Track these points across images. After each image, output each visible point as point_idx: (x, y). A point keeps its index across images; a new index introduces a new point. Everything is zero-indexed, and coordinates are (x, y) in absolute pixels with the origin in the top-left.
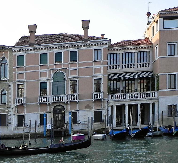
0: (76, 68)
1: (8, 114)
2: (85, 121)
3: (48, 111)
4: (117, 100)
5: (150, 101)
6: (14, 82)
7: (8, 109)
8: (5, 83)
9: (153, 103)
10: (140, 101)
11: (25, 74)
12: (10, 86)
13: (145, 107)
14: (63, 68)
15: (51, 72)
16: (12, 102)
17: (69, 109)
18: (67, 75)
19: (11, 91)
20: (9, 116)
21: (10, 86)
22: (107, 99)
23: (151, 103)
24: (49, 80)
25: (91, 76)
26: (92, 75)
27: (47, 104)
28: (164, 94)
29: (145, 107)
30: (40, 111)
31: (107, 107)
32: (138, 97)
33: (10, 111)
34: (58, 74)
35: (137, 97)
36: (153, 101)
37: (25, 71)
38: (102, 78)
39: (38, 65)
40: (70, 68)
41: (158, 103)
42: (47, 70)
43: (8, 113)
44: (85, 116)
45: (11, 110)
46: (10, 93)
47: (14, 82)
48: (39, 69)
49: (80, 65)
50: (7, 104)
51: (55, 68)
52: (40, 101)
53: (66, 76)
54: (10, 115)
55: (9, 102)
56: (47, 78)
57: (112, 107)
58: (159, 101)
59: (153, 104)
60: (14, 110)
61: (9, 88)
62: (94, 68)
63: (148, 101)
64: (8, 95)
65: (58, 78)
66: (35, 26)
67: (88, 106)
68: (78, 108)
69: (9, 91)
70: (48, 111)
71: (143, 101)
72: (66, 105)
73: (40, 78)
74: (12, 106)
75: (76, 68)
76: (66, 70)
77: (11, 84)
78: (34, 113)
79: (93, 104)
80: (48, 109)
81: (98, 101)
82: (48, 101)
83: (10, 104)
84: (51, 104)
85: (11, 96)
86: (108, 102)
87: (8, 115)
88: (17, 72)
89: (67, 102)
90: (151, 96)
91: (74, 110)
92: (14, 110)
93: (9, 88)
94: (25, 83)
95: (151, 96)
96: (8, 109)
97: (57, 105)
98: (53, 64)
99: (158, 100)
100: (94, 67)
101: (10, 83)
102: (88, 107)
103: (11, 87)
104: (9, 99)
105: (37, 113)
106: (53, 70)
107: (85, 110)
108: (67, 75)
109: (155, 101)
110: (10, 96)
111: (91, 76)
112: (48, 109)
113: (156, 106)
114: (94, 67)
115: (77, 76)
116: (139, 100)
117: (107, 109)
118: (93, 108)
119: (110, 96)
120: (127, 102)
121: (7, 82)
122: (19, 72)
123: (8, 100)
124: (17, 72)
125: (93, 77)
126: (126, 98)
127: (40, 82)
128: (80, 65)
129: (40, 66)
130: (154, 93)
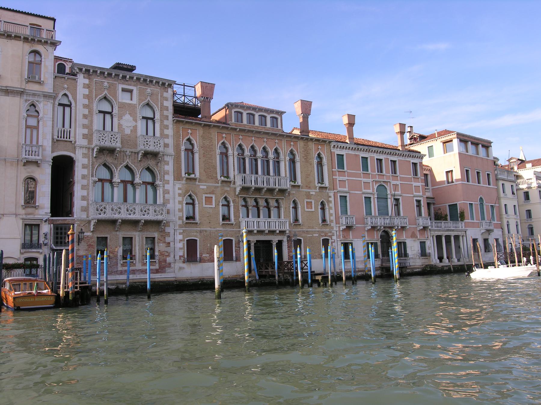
6: (335, 191)
12: (330, 197)
14: (385, 180)
16: (334, 221)
19: (332, 205)
24: (373, 194)
26: (413, 194)
33: (334, 235)
37: (346, 178)
42: (370, 180)
43: (331, 236)
46: (330, 208)
47: (335, 191)
49: (402, 179)
51: (377, 179)
53: (389, 192)
55: (331, 221)
61: (330, 199)
64: (329, 211)
66: (310, 103)
83: (332, 225)
88: (338, 178)
93: (330, 199)
94: (348, 195)
103: (332, 199)
106: (376, 182)
122: (341, 177)
123: (330, 218)
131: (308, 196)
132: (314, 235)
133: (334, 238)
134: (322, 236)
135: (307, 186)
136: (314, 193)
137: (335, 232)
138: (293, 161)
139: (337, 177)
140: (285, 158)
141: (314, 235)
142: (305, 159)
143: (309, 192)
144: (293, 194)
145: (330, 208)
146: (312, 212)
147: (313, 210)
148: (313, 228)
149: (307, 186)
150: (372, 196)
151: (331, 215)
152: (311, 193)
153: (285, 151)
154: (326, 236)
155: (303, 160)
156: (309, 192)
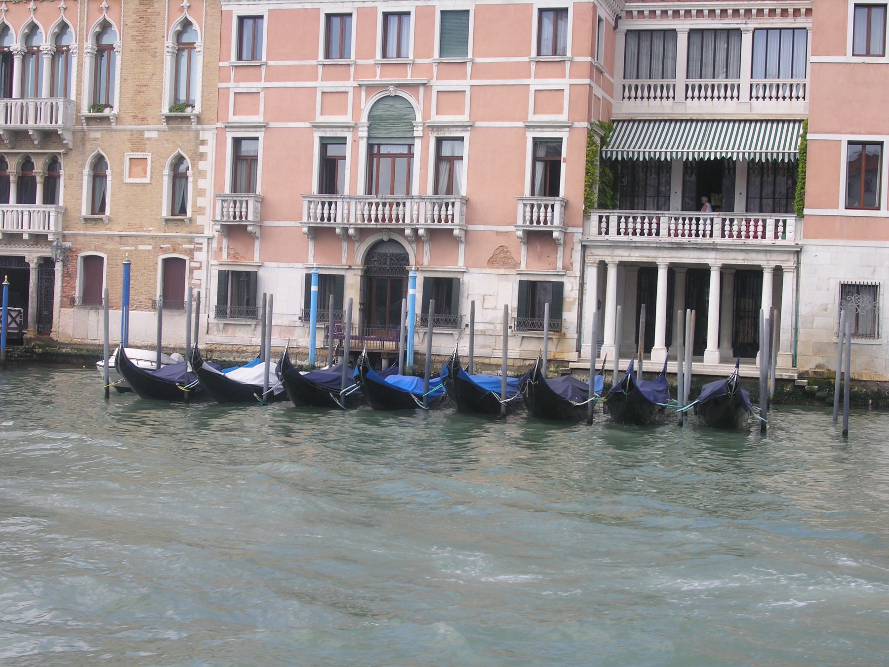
0: (463, 84)
1: (192, 259)
2: (488, 320)
3: (344, 261)
4: (622, 238)
5: (761, 256)
7: (191, 240)
8: (184, 126)
9: (773, 264)
10: (719, 255)
11: (262, 95)
12: (203, 142)
13: (744, 283)
15: (363, 94)
17: (426, 261)
18: (426, 114)
20: (196, 268)
21: (203, 142)
22: (580, 230)
23: (767, 263)
24: (354, 128)
25: (521, 124)
26: (524, 118)
27: (338, 231)
28: (827, 229)
29: (744, 283)
30: (313, 260)
31: (577, 267)
32: (711, 236)
33: (200, 249)
34: (390, 102)
35: (708, 233)
36: (774, 257)
37: (263, 84)
38: (564, 134)
39: (314, 62)
40: (439, 85)
41: (797, 268)
42: (349, 85)
43: (191, 253)
44: (490, 295)
45: (205, 246)
46: (201, 174)
48: (316, 79)
50: (191, 220)
51: (378, 79)
52: (309, 216)
53: (419, 118)
54: (198, 265)
55: (200, 211)
56: (347, 119)
57: (603, 267)
58: (804, 258)
59: (778, 272)
60: (215, 244)
61: (202, 149)
62: (532, 89)
63: (754, 256)
64: (195, 182)
65: (389, 122)
67: (502, 255)
68: (461, 263)
69: (202, 165)
70: (344, 261)
71: (732, 255)
72: (414, 245)
73: (320, 119)
74: (211, 230)
75: (463, 84)
76: (422, 89)
77: (209, 135)
78: (291, 265)
79: (523, 249)
80: (344, 255)
81: (538, 238)
82: (339, 220)
83: (200, 220)
84: (351, 232)
85: (208, 184)
86: (584, 247)
87: (193, 265)
88: (234, 86)
89: (416, 231)
90: (770, 233)
91: (443, 269)
92: (215, 244)
93: (202, 149)
95: (770, 233)
96: (191, 240)
97: (380, 243)
98: (371, 62)
99: (798, 253)
100: (535, 83)
101: (203, 130)
102: (500, 259)
104: (199, 199)
105: (300, 265)
106: (370, 88)
107: (489, 271)
108: (426, 114)
109: (785, 257)
110: (202, 184)
111: (521, 124)
112: (344, 255)
113: (788, 280)
114: (535, 83)
115: (464, 118)
116: (714, 248)
117: (578, 274)
118: (523, 267)
119: (594, 218)
120: (666, 254)
121: (194, 126)
122: (242, 84)
124: (234, 86)
125: (527, 127)
126: (663, 231)
127: (317, 135)
128: (479, 71)
129: (320, 69)
130: (781, 223)
131: (138, 142)
132: (141, 247)
133: (200, 256)
134: (165, 251)
135: (135, 117)
136: (154, 135)
137: (205, 241)
138: (102, 52)
139: (231, 84)
140: (81, 48)
141: (141, 247)
142: (139, 42)
143: (141, 132)
144: (96, 139)
145: (201, 174)
146: (144, 185)
147: (147, 180)
148: (141, 227)
149: (135, 117)
150: (349, 135)
151: (201, 193)
152: (147, 135)
153: (81, 29)
154: (174, 250)
155: (133, 45)
156: (141, 132)
